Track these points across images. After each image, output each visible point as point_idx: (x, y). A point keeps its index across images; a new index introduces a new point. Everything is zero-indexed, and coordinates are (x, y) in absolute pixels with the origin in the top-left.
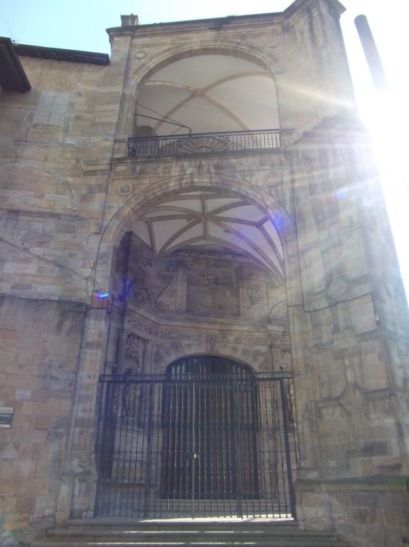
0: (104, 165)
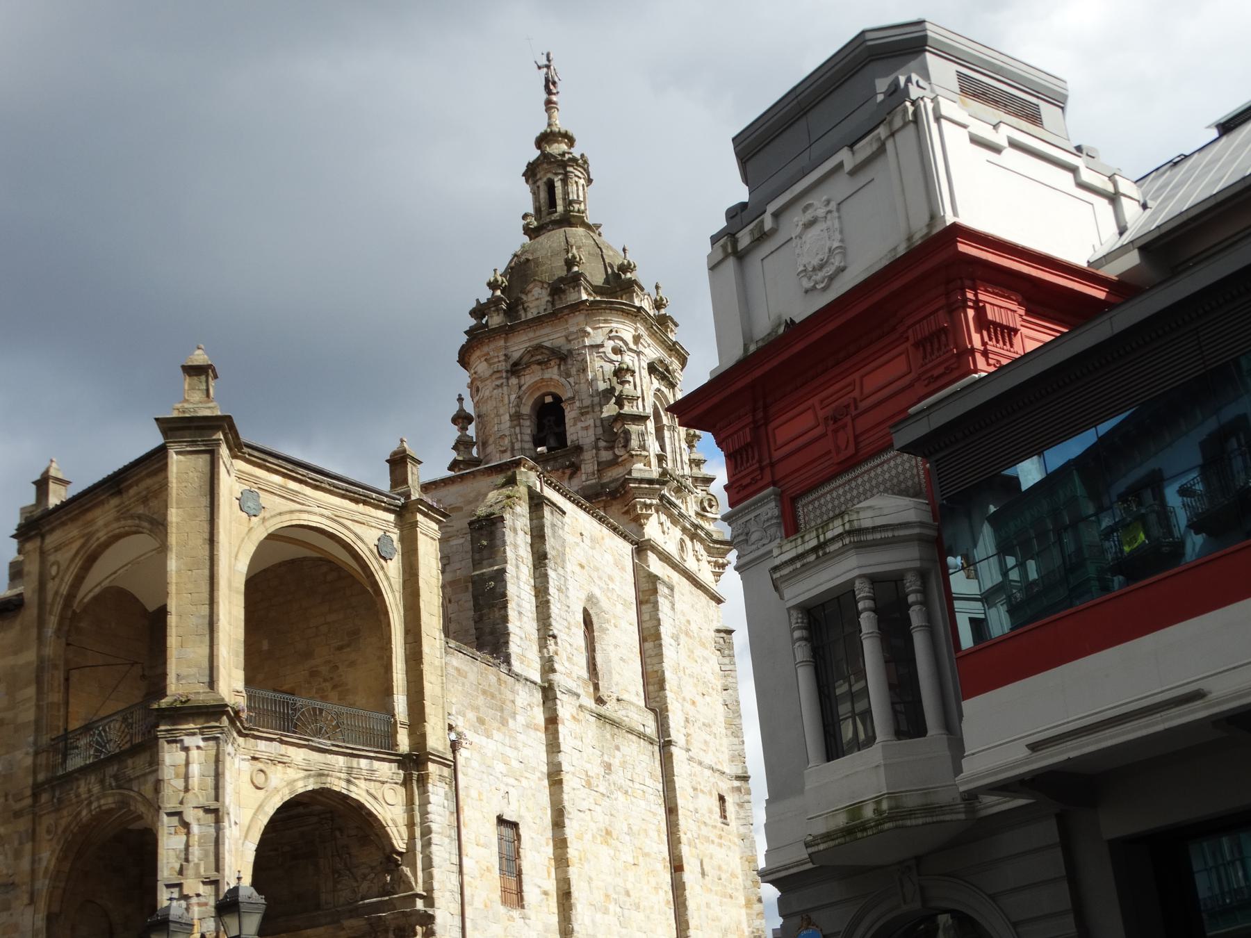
0: (28, 801)
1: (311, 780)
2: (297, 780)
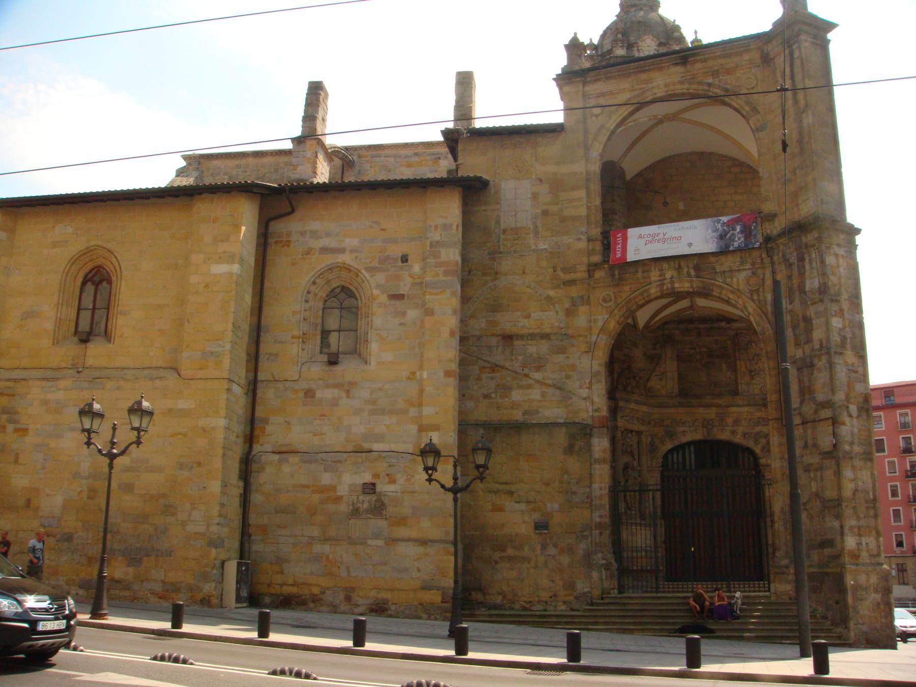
0: (581, 274)
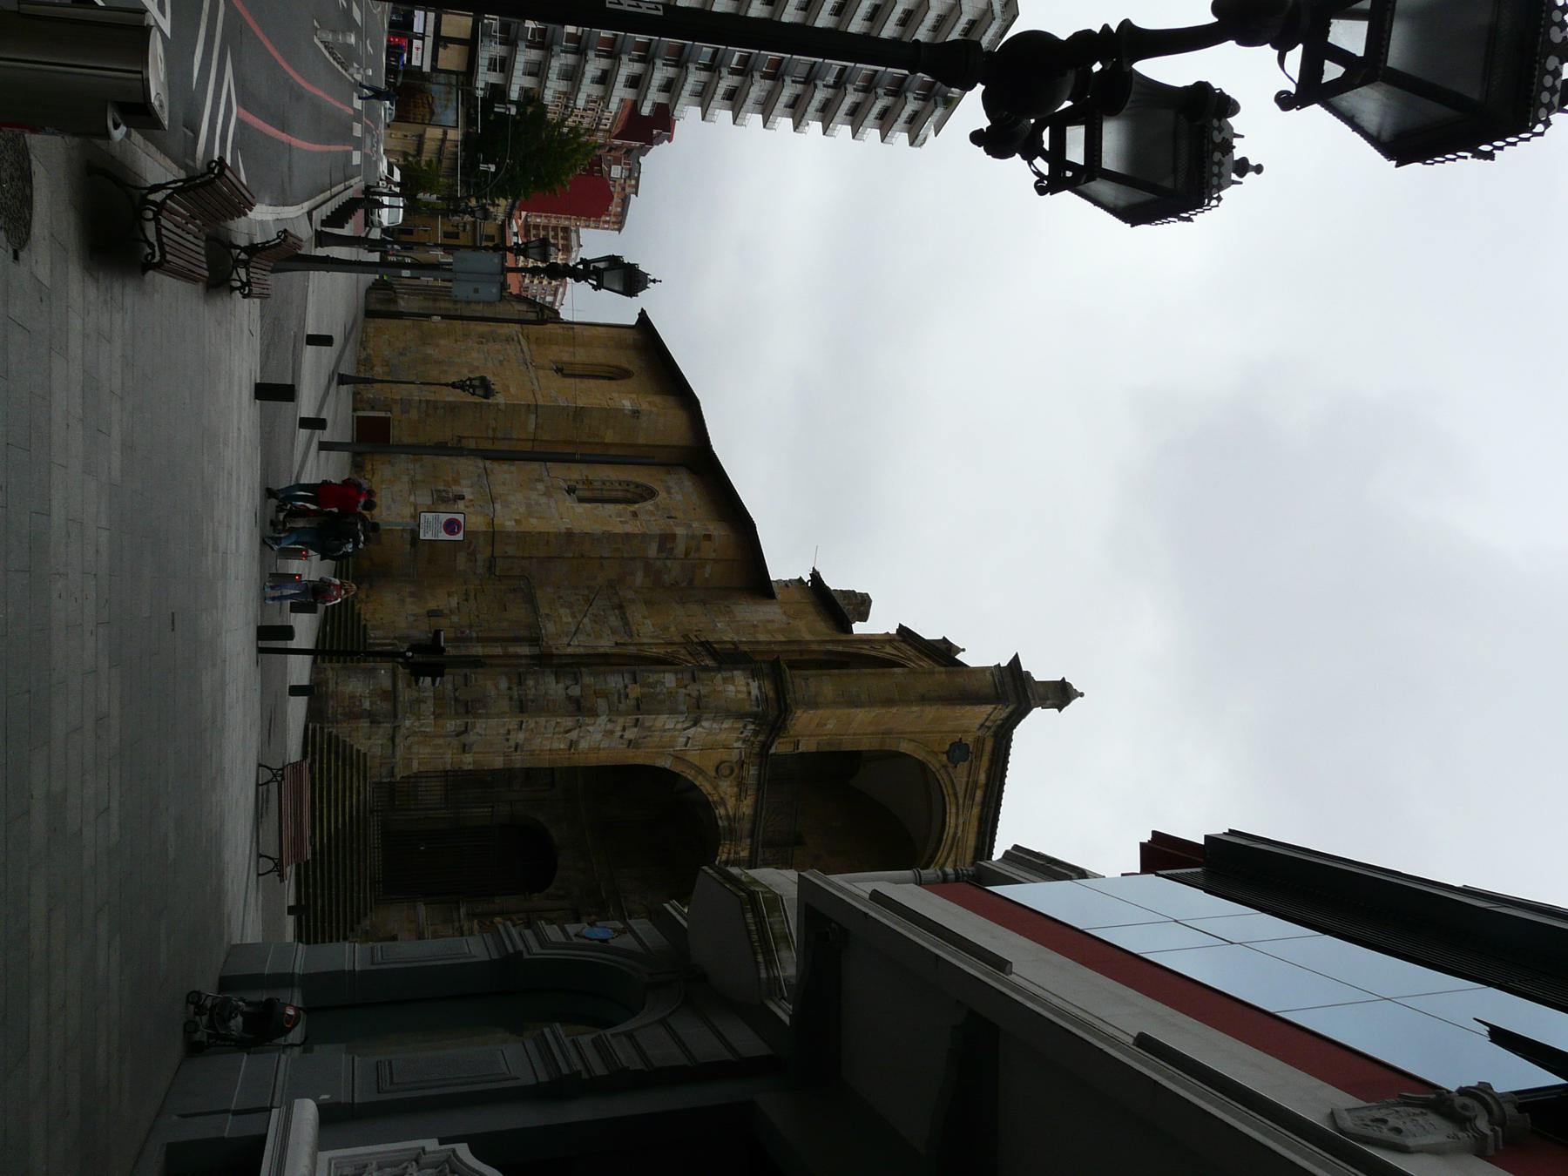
1: (726, 823)
2: (726, 809)
